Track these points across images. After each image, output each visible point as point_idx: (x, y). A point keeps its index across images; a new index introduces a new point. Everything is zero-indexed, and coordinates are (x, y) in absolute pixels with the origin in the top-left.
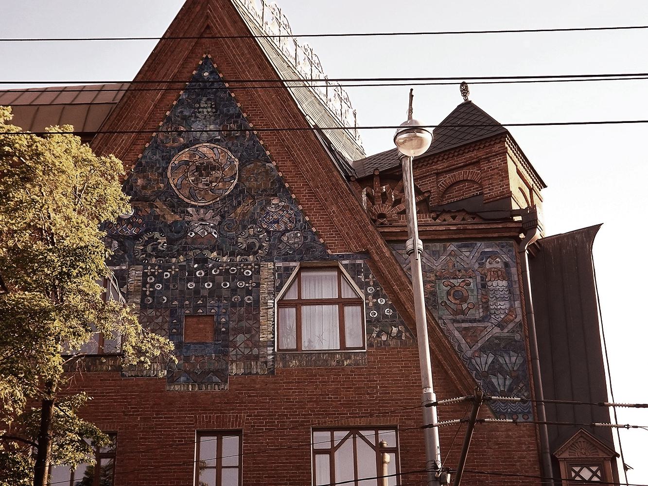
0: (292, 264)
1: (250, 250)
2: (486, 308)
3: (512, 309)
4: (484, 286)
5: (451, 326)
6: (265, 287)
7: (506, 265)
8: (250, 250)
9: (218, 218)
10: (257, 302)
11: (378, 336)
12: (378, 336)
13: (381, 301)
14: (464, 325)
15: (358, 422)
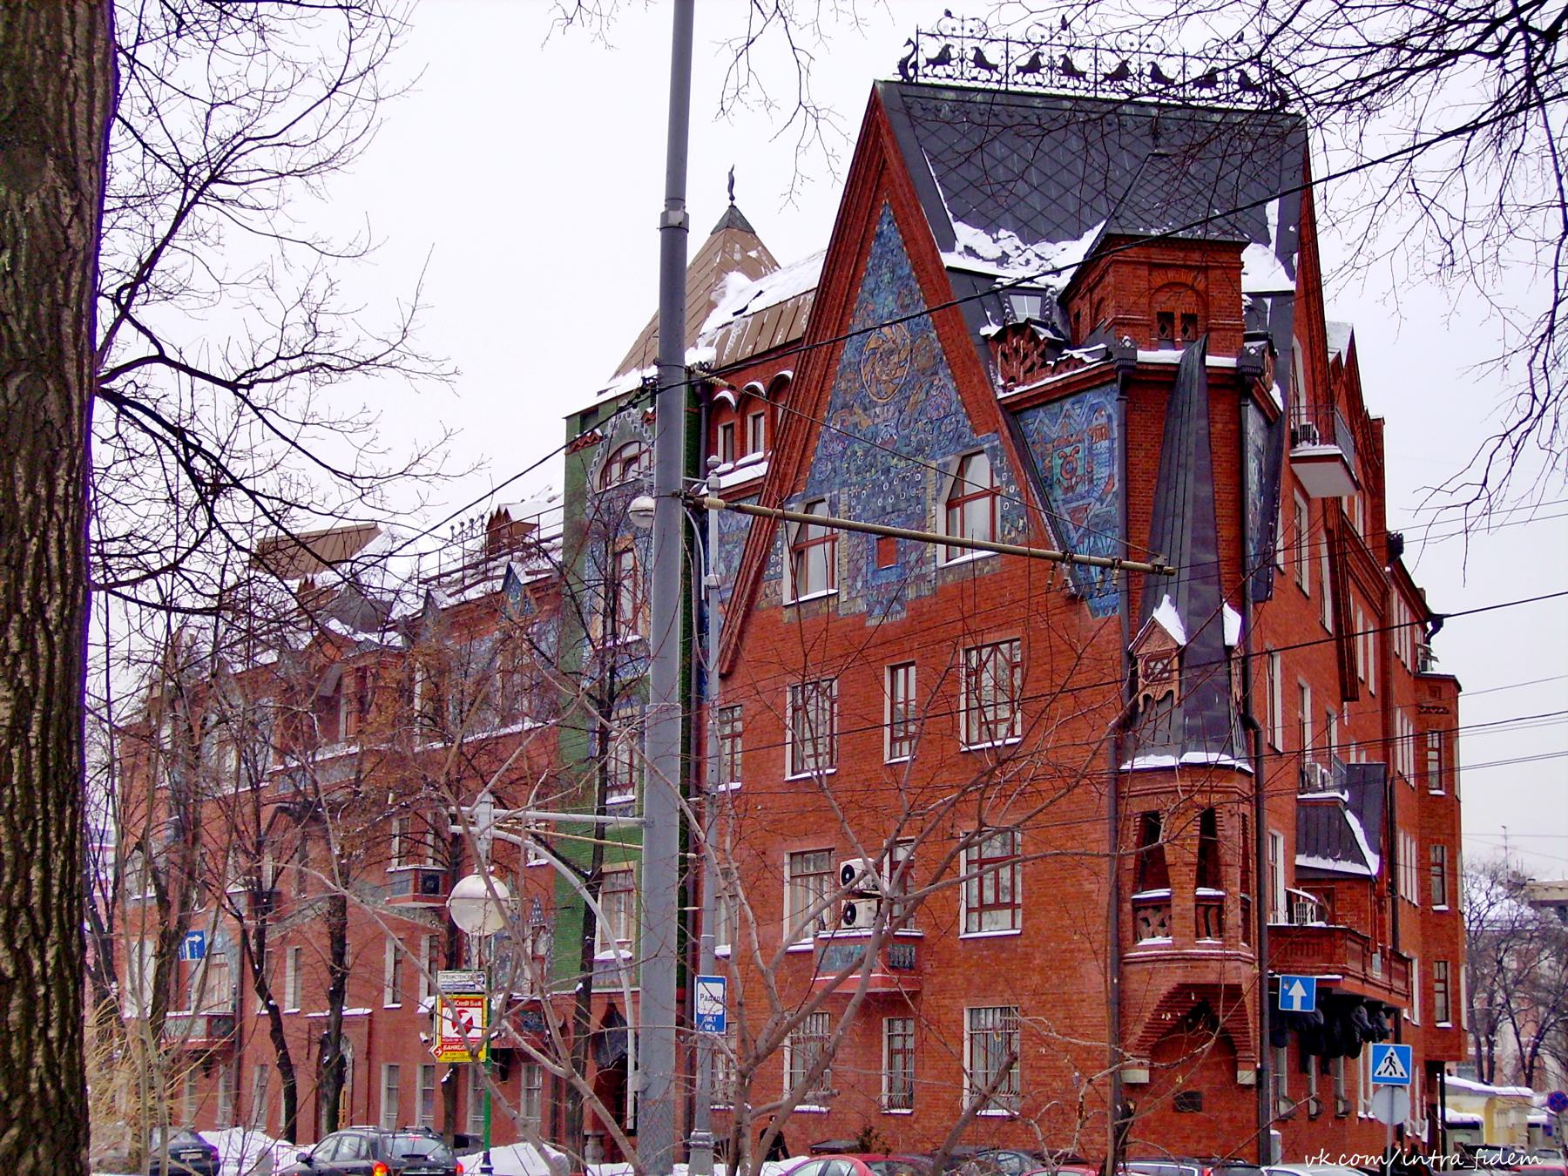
0: (950, 458)
1: (919, 450)
2: (1091, 481)
3: (1111, 476)
4: (1090, 449)
5: (1063, 510)
6: (931, 491)
7: (1109, 417)
8: (919, 450)
9: (897, 414)
10: (924, 510)
11: (1009, 533)
12: (1009, 533)
13: (1012, 489)
14: (1074, 505)
15: (991, 638)
